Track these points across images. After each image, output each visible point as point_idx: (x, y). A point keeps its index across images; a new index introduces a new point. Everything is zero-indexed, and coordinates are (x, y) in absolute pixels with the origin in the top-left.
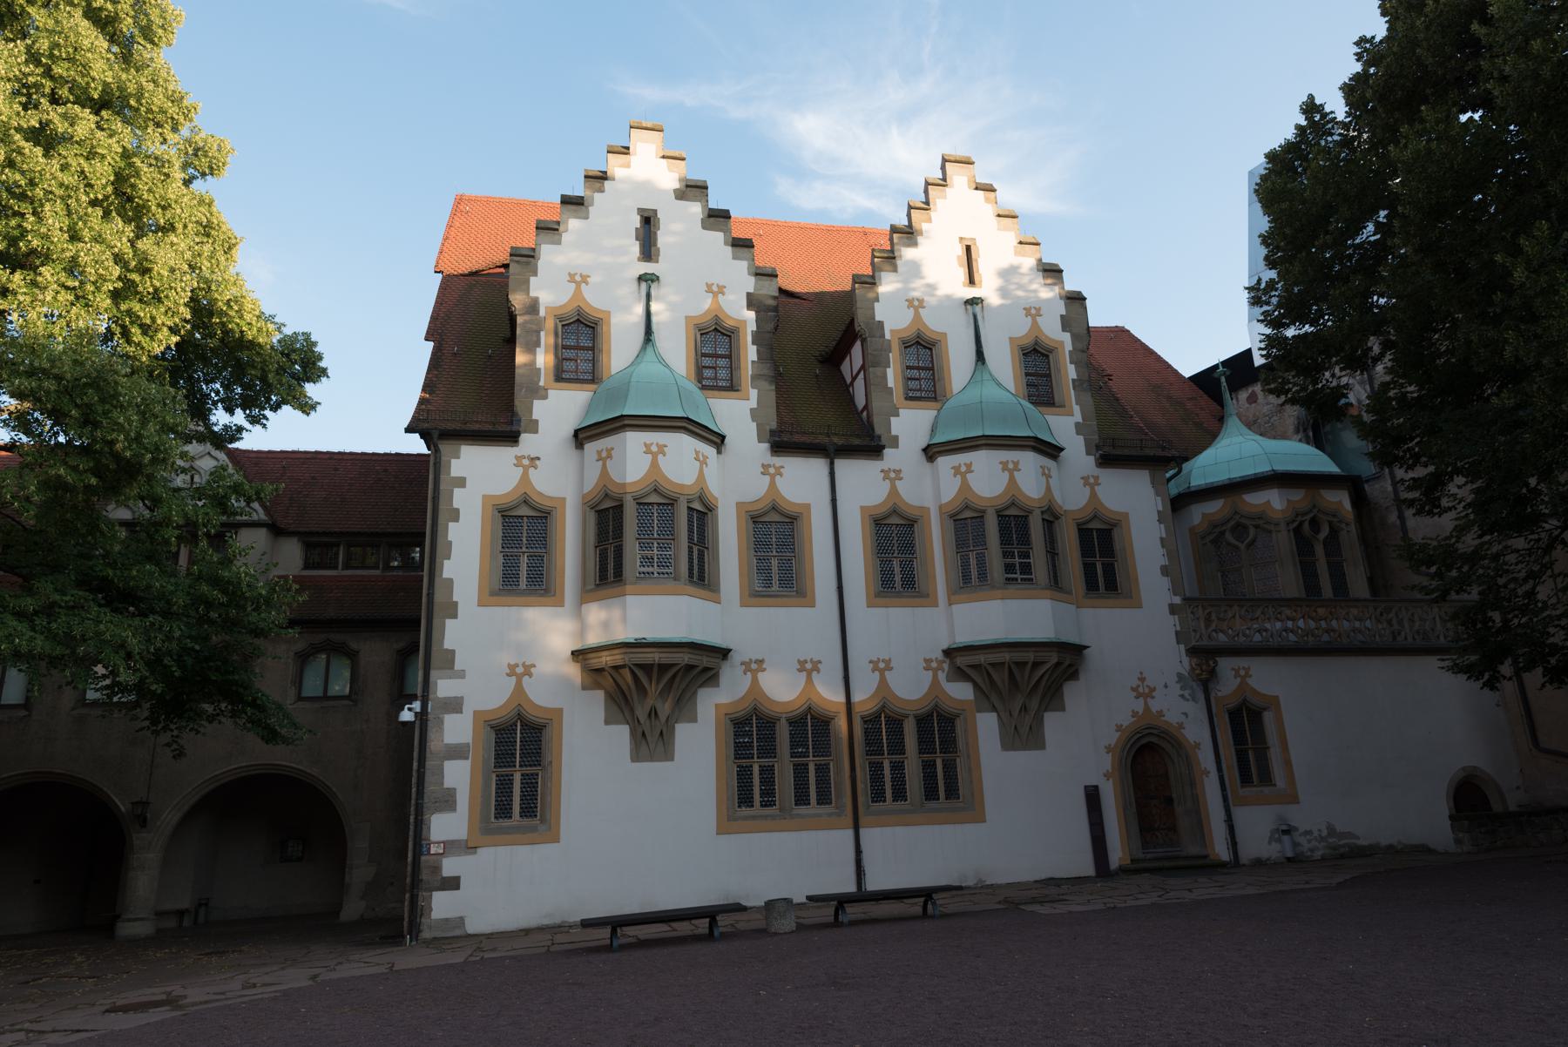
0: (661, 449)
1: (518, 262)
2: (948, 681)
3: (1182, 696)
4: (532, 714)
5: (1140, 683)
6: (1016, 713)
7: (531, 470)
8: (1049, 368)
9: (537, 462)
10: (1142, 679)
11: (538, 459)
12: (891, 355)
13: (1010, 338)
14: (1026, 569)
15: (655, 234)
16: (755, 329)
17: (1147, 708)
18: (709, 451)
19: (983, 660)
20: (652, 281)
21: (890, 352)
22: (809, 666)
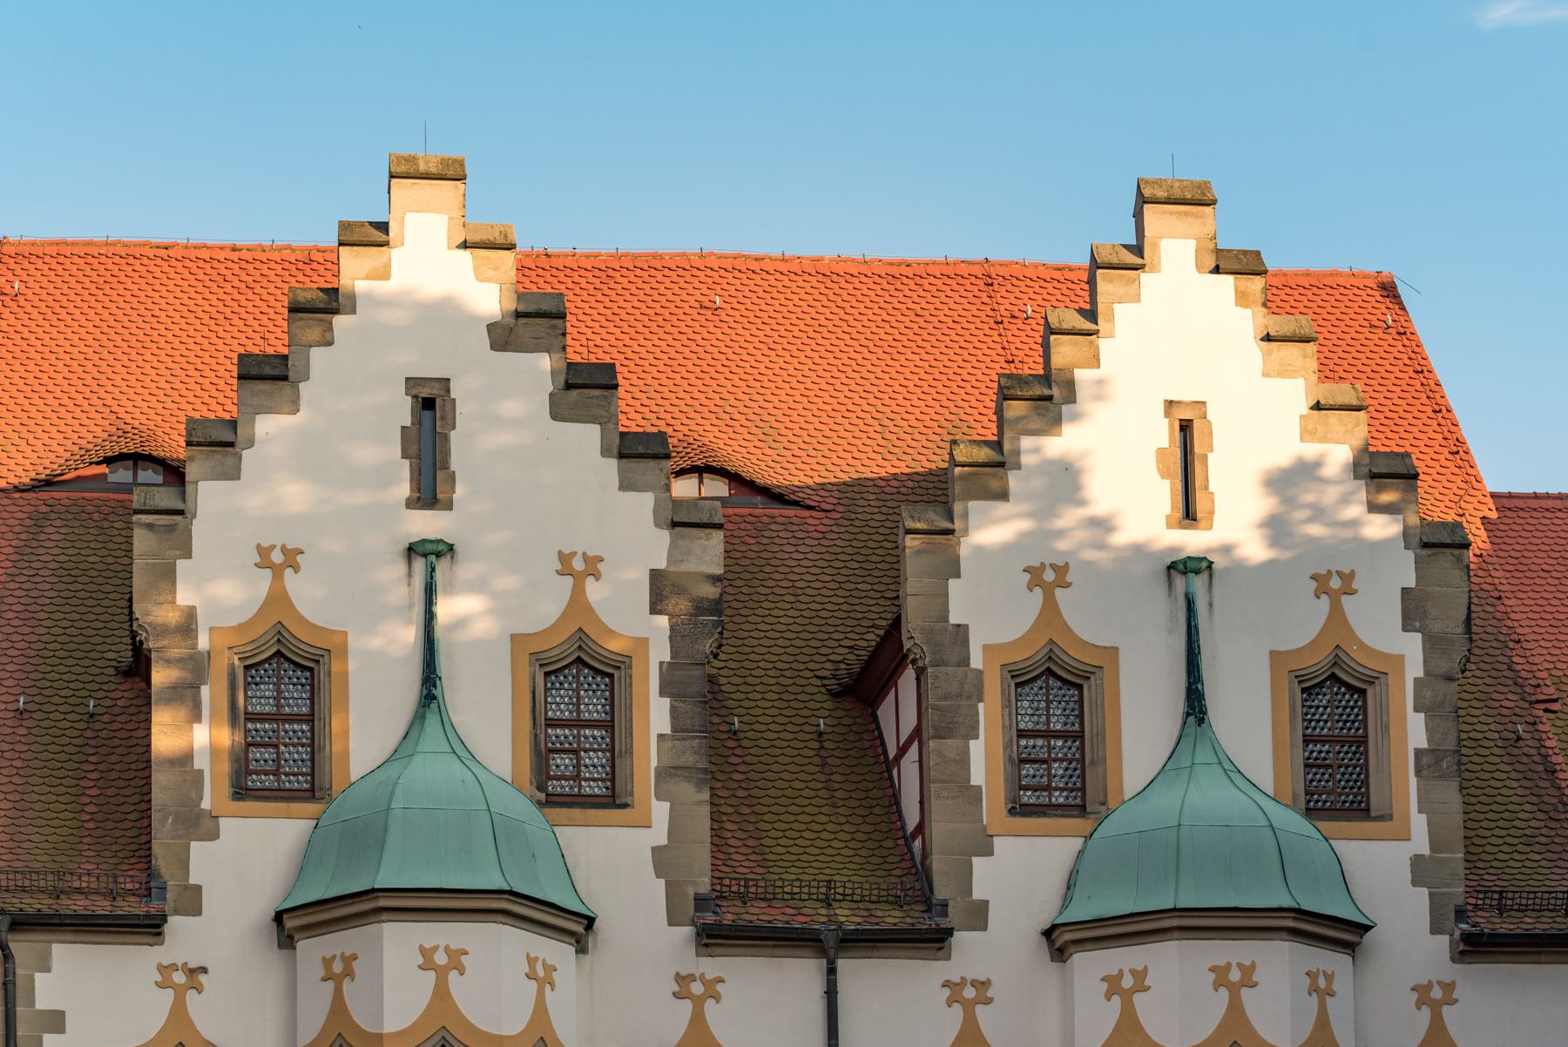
0: (456, 960)
1: (150, 526)
7: (191, 995)
8: (1365, 721)
9: (202, 978)
11: (204, 970)
12: (981, 706)
16: (667, 659)
18: (557, 952)
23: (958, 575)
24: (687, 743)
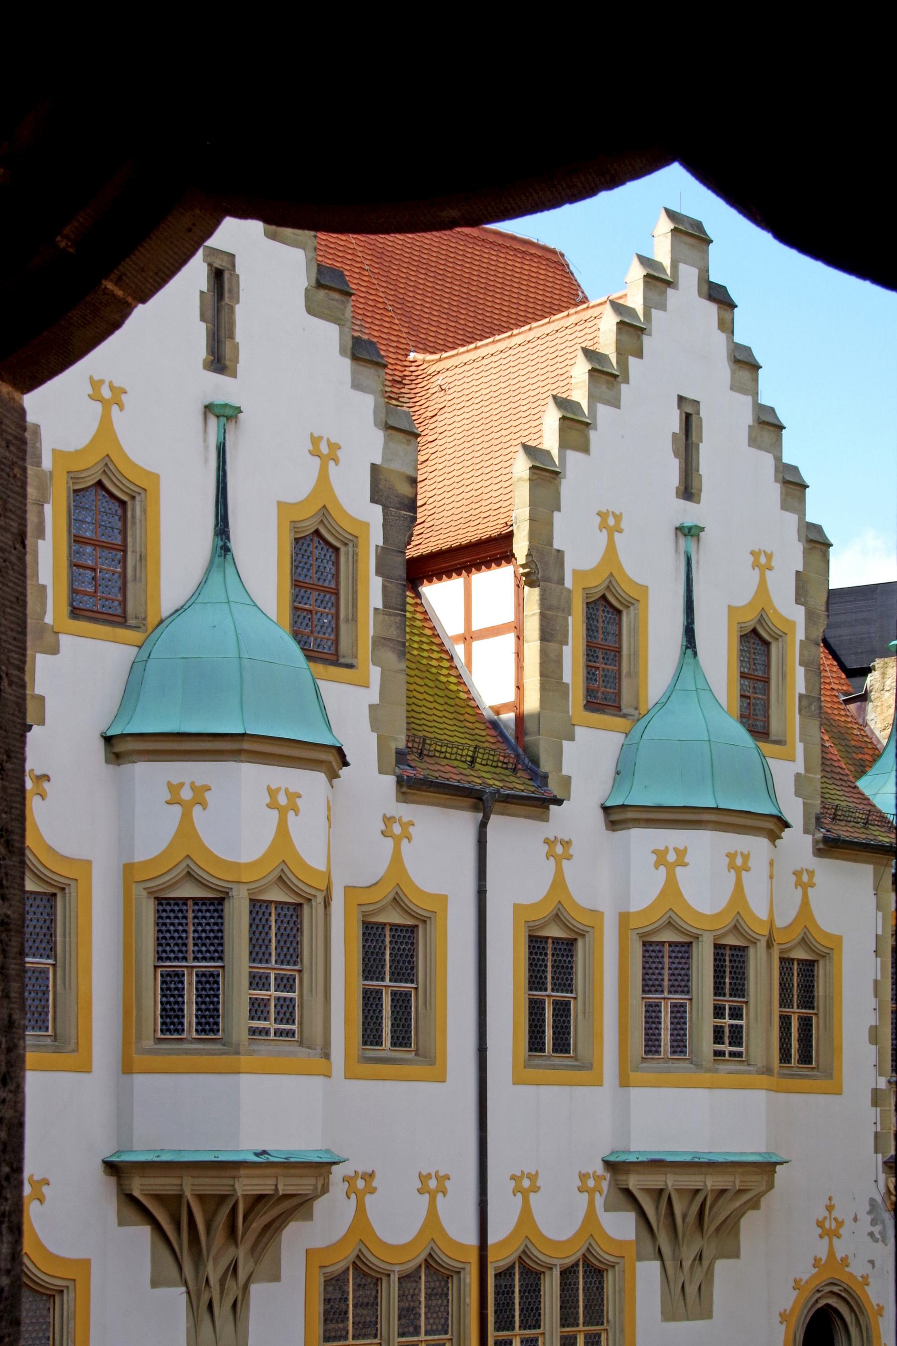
2: (606, 1210)
3: (871, 1234)
5: (827, 1214)
6: (687, 1264)
8: (768, 666)
9: (46, 785)
10: (830, 1208)
12: (570, 618)
13: (730, 608)
14: (736, 1037)
15: (232, 310)
16: (381, 544)
17: (831, 1253)
19: (670, 1184)
20: (228, 418)
21: (570, 615)
22: (433, 1184)
23: (559, 510)
24: (392, 618)
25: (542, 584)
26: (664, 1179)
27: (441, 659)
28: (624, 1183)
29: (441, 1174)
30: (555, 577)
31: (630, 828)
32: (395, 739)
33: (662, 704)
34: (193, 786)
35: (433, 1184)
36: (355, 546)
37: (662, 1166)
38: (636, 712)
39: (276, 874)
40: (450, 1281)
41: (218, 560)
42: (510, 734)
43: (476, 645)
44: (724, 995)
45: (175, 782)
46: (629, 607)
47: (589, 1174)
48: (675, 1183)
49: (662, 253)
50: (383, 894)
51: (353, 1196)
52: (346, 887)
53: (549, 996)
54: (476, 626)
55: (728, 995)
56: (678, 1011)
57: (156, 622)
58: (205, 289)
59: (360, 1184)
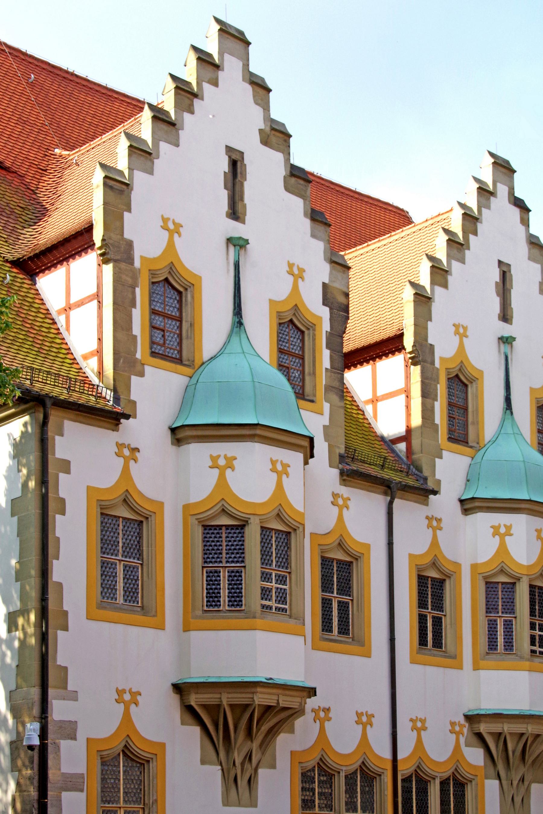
2: (466, 746)
4: (138, 747)
6: (515, 783)
9: (137, 454)
12: (438, 386)
13: (531, 389)
15: (242, 185)
16: (329, 330)
19: (506, 729)
20: (241, 247)
21: (438, 383)
24: (336, 375)
25: (422, 363)
26: (502, 726)
27: (358, 414)
28: (477, 729)
29: (369, 713)
30: (429, 360)
31: (477, 512)
32: (339, 447)
33: (493, 441)
34: (226, 457)
35: (364, 719)
36: (314, 330)
37: (501, 718)
38: (478, 445)
39: (276, 512)
40: (374, 780)
41: (235, 329)
42: (403, 455)
43: (379, 404)
44: (535, 616)
45: (215, 455)
46: (472, 383)
47: (455, 722)
48: (509, 729)
49: (487, 177)
50: (332, 540)
51: (318, 721)
52: (311, 533)
53: (430, 613)
54: (379, 394)
55: (537, 617)
56: (508, 625)
57: (200, 363)
58: (227, 171)
59: (322, 714)
